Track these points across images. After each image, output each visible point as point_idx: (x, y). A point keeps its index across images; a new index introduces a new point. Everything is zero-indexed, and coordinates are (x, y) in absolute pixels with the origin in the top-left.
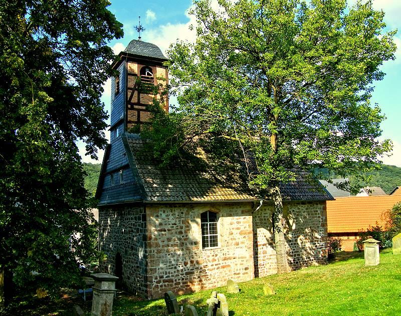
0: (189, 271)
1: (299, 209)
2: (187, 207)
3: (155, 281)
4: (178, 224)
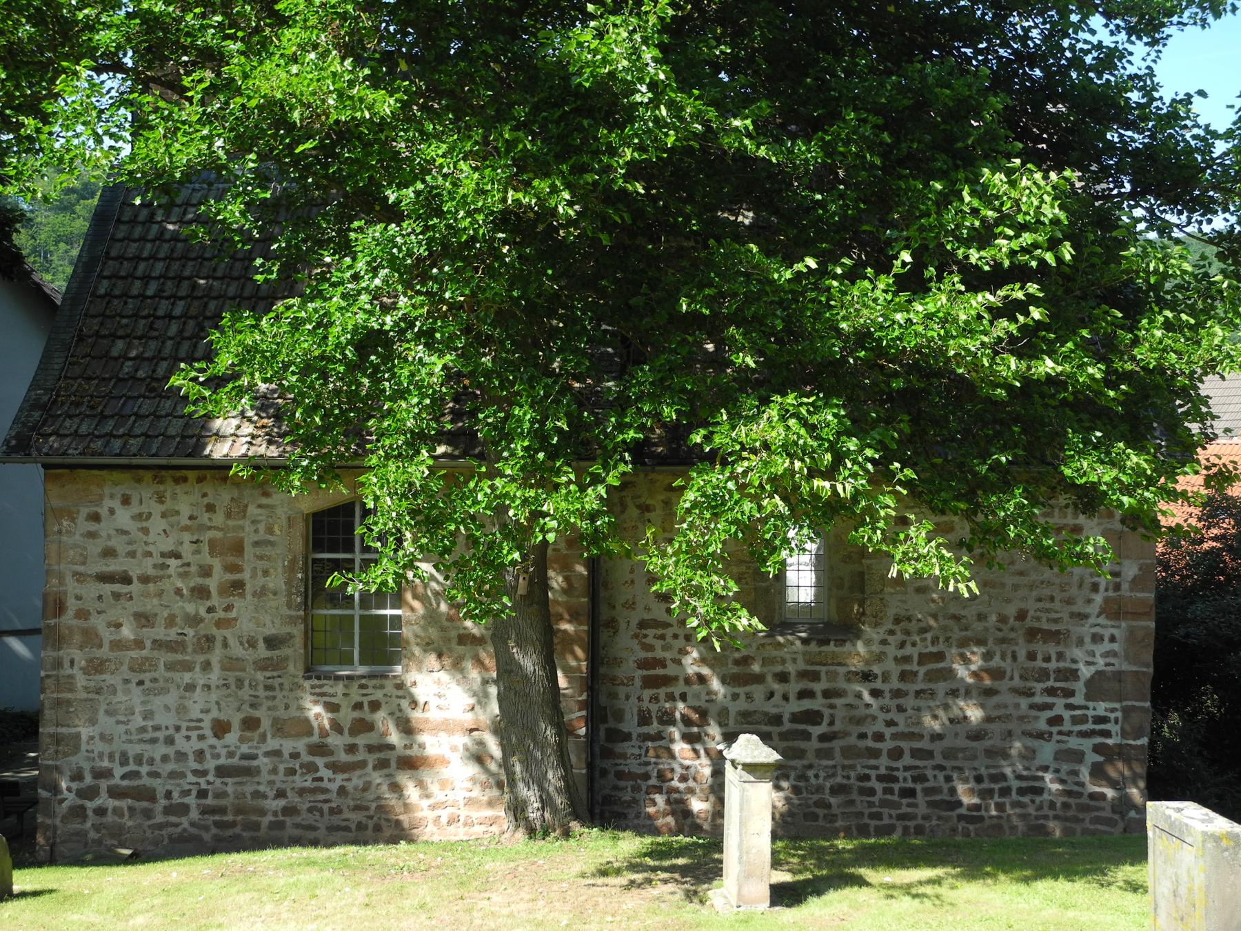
0: (235, 761)
3: (75, 786)
4: (187, 555)
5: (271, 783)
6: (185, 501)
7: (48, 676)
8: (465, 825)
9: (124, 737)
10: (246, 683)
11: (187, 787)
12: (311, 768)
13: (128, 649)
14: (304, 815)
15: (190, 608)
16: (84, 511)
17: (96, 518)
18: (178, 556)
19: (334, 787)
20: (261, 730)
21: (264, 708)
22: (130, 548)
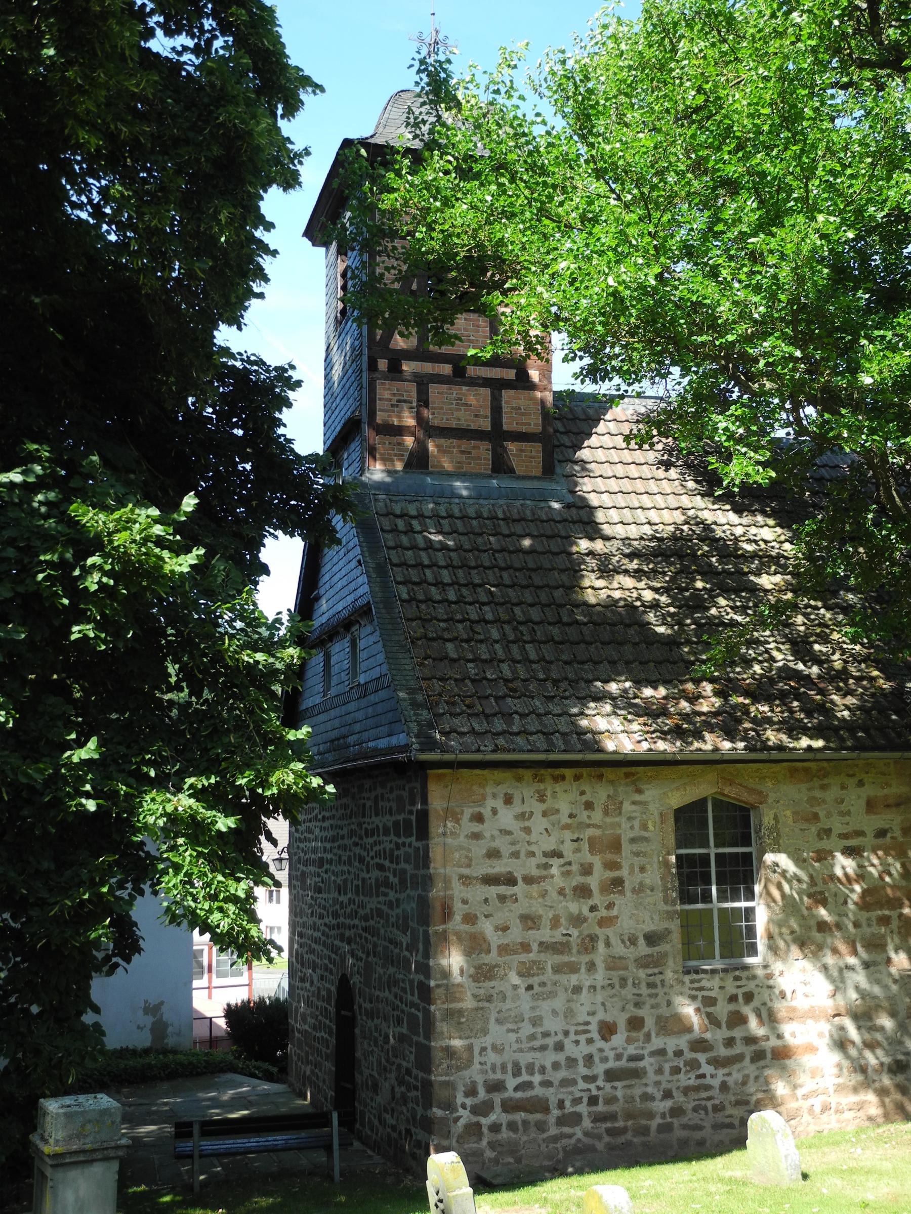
0: (623, 1063)
2: (612, 782)
3: (469, 1102)
4: (569, 855)
5: (657, 1083)
6: (565, 798)
7: (438, 986)
8: (837, 1111)
9: (515, 1046)
10: (630, 982)
11: (578, 1095)
12: (694, 1065)
13: (515, 952)
14: (690, 1114)
15: (574, 907)
16: (468, 812)
17: (479, 818)
18: (560, 855)
19: (716, 1083)
20: (646, 1029)
21: (647, 1006)
22: (514, 848)
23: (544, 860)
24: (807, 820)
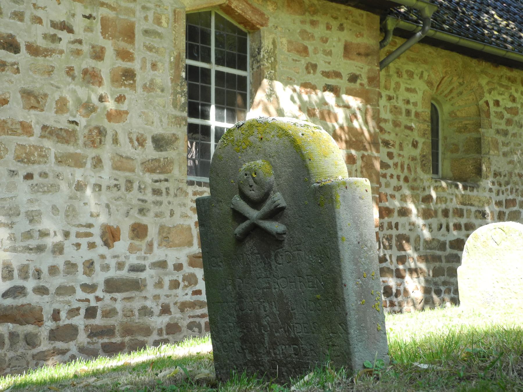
0: (124, 273)
1: (514, 100)
4: (80, 32)
5: (156, 297)
10: (136, 185)
11: (76, 305)
13: (14, 132)
18: (70, 30)
20: (148, 239)
21: (151, 214)
23: (52, 31)
24: (298, 52)
